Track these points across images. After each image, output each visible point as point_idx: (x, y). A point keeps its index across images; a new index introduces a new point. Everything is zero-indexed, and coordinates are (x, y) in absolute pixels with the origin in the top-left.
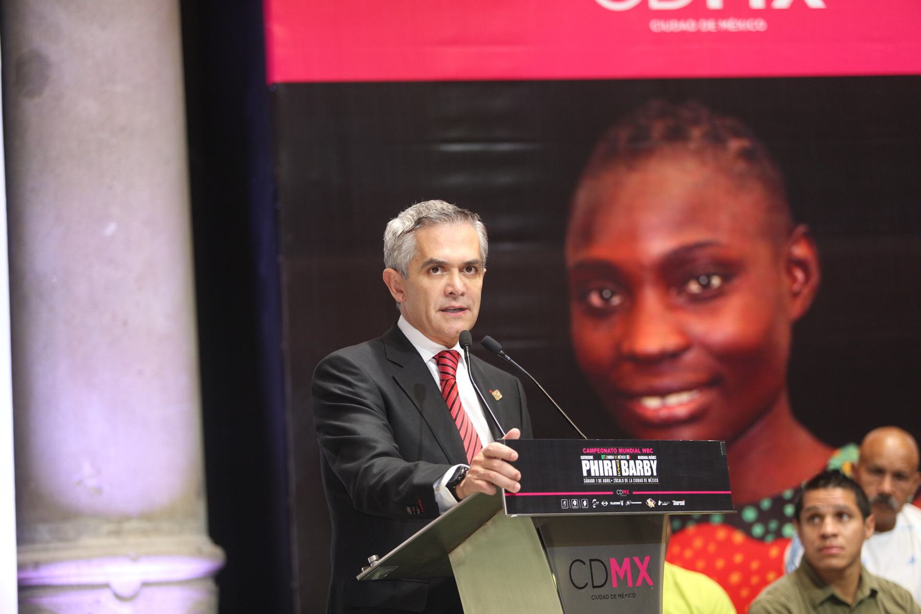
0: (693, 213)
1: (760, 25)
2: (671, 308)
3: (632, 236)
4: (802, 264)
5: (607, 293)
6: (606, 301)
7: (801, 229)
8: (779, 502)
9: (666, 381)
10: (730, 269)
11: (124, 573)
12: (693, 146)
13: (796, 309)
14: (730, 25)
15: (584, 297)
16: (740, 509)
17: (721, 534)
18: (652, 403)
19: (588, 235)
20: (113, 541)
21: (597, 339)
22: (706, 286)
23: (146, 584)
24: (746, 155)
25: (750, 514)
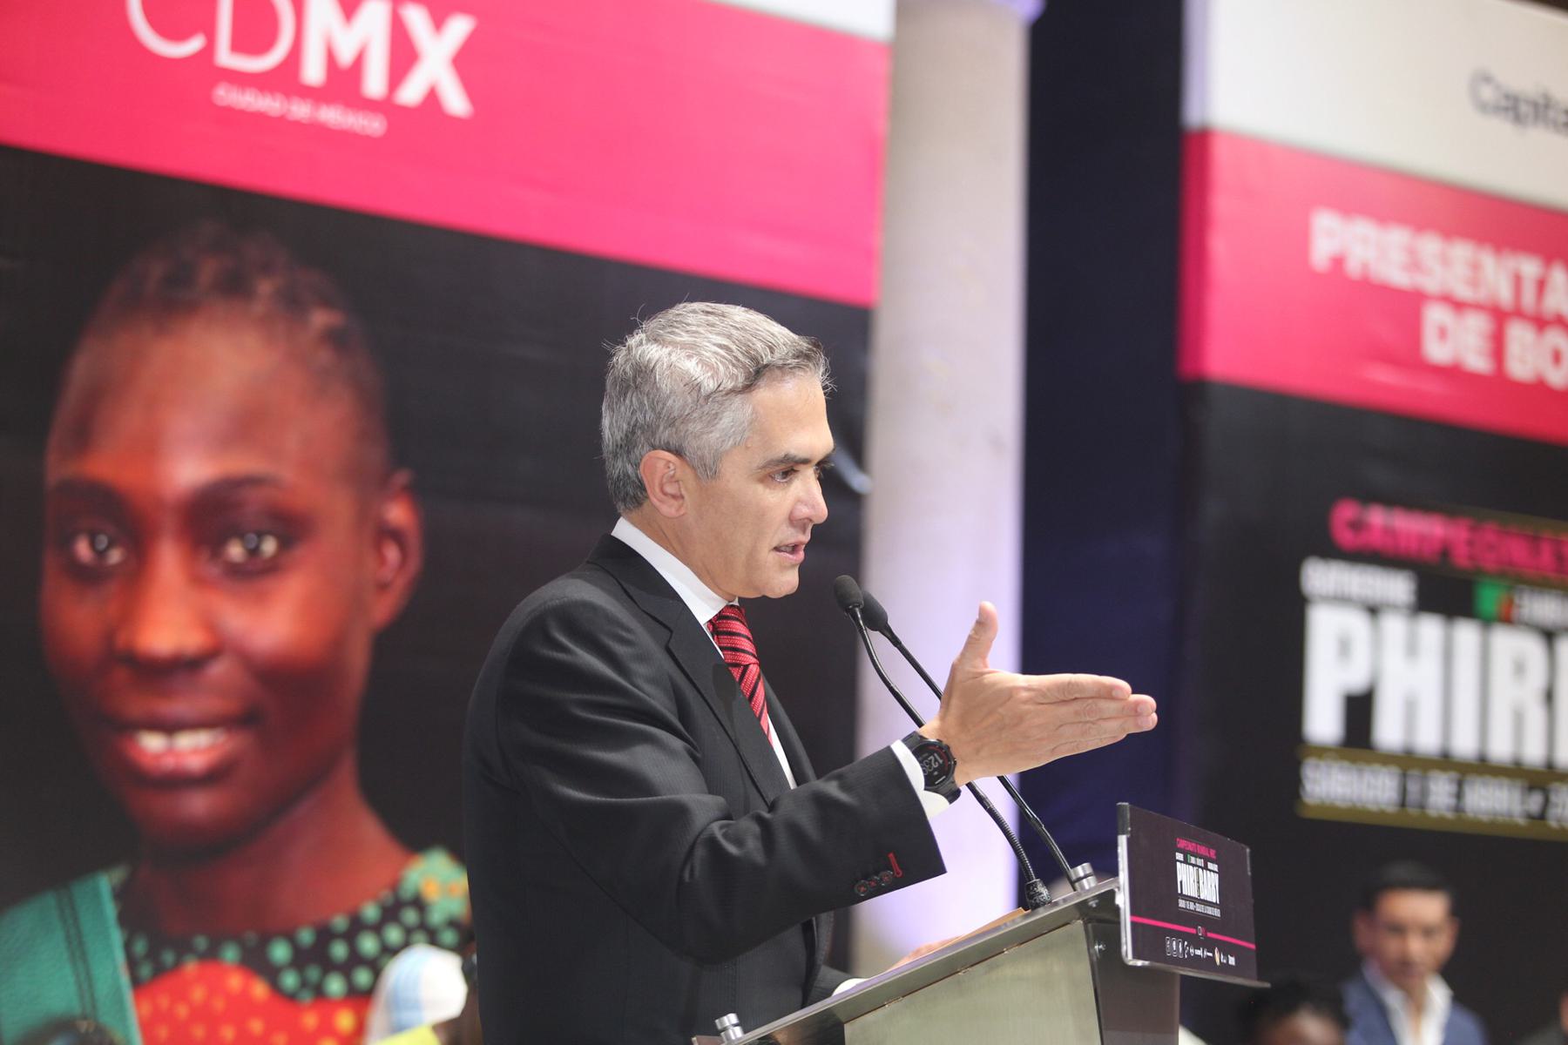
0: (247, 424)
1: (373, 125)
2: (198, 581)
3: (150, 448)
4: (396, 535)
5: (103, 541)
6: (101, 555)
7: (402, 478)
8: (325, 935)
10: (292, 527)
12: (258, 308)
13: (382, 609)
15: (67, 542)
16: (265, 940)
17: (235, 982)
18: (152, 743)
19: (83, 437)
21: (78, 618)
22: (254, 552)
24: (334, 338)
25: (280, 952)
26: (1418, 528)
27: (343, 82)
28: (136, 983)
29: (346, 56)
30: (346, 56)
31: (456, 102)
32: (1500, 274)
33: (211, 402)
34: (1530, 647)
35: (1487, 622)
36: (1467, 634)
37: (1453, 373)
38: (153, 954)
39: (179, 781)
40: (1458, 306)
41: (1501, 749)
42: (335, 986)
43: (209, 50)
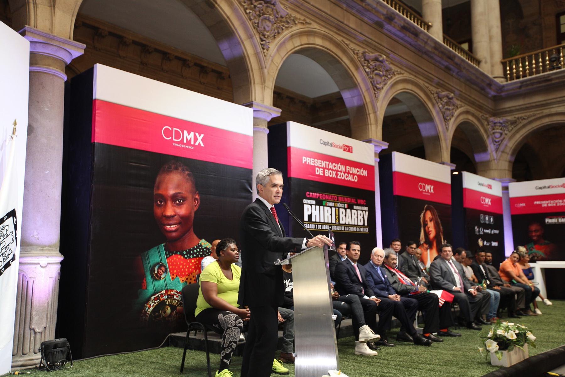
0: (178, 186)
1: (193, 148)
2: (173, 206)
3: (167, 189)
4: (197, 199)
6: (161, 203)
9: (171, 222)
10: (184, 199)
11: (43, 261)
13: (195, 209)
14: (187, 147)
17: (179, 257)
18: (168, 227)
19: (158, 188)
20: (41, 252)
21: (158, 211)
23: (49, 264)
24: (188, 175)
25: (185, 253)
26: (316, 195)
27: (189, 142)
28: (167, 257)
29: (189, 139)
30: (189, 139)
31: (202, 145)
32: (324, 164)
33: (174, 183)
34: (329, 208)
35: (324, 206)
36: (322, 207)
37: (319, 175)
38: (169, 254)
39: (172, 231)
40: (319, 168)
41: (326, 221)
42: (191, 257)
43: (172, 138)
